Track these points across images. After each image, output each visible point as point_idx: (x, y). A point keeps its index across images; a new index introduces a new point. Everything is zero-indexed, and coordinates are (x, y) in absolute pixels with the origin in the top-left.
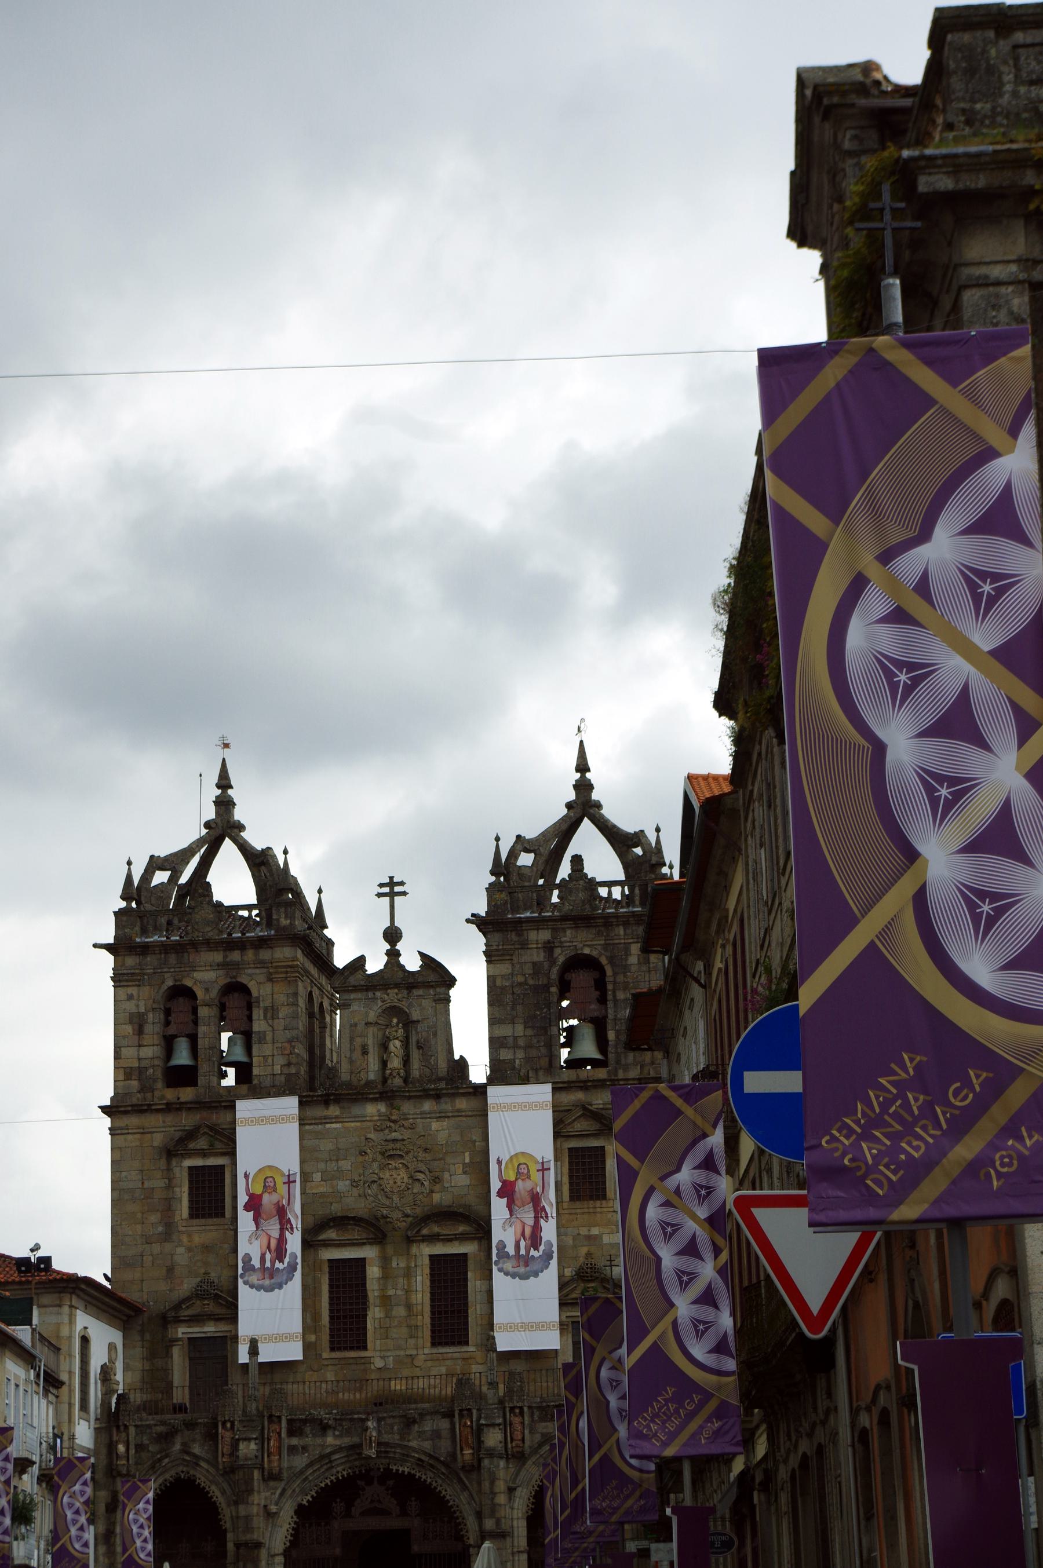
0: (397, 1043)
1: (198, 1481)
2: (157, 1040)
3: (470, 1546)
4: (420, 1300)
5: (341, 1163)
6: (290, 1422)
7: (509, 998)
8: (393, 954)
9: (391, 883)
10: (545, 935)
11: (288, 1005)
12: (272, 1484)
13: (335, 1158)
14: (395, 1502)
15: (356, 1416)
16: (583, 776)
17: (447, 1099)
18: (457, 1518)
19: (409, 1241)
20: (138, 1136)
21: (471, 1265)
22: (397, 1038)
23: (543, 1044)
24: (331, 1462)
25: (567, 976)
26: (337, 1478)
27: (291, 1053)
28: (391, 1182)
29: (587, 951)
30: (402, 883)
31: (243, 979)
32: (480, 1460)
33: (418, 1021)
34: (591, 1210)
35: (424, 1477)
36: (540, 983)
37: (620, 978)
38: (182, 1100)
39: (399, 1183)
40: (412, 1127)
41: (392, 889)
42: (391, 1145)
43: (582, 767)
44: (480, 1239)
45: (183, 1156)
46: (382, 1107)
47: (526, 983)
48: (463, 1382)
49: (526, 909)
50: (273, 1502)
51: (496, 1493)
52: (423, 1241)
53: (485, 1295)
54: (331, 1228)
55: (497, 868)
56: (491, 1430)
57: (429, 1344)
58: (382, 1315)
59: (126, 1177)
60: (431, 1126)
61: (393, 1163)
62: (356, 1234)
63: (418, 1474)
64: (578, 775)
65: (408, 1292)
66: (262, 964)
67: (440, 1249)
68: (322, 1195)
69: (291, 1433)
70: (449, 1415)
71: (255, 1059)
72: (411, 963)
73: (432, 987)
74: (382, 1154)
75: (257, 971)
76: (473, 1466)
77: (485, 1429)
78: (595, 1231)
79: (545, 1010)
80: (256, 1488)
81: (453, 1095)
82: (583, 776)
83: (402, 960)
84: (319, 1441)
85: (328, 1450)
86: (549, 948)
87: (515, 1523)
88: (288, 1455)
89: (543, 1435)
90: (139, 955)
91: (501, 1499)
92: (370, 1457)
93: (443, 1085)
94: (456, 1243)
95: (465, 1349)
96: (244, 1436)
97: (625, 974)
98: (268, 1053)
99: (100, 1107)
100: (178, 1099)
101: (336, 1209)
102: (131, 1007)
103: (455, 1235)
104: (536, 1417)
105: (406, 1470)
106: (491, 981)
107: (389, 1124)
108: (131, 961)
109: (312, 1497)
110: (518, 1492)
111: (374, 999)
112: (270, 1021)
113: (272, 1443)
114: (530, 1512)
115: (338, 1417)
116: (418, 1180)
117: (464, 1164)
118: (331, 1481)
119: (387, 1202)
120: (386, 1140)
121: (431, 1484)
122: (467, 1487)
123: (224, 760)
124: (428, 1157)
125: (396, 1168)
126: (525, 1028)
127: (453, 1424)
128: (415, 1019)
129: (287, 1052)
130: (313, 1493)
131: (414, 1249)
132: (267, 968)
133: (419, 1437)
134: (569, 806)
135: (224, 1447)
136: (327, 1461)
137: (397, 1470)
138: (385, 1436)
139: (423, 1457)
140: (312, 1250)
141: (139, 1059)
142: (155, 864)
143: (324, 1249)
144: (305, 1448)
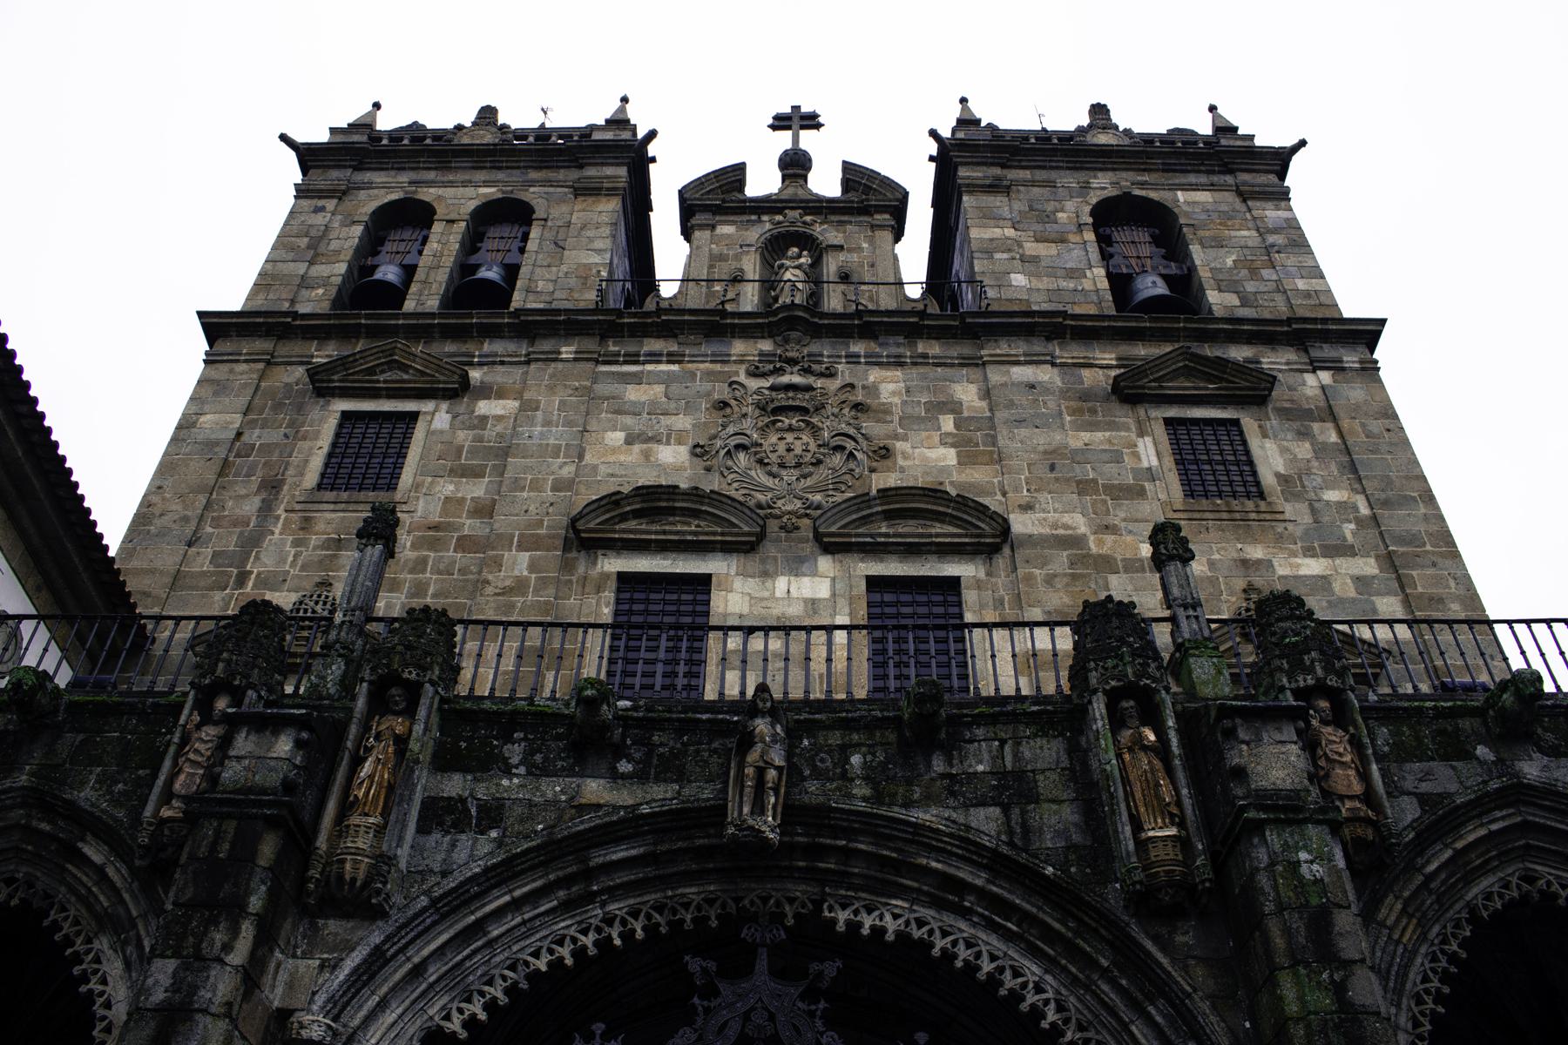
0: (797, 272)
12: (333, 927)
17: (901, 340)
20: (261, 366)
24: (588, 874)
25: (1101, 230)
28: (782, 447)
29: (1137, 192)
33: (841, 248)
34: (1237, 516)
35: (963, 953)
40: (830, 374)
46: (766, 346)
50: (320, 999)
51: (1348, 964)
62: (688, 528)
63: (940, 943)
73: (865, 210)
74: (762, 407)
78: (1256, 552)
88: (423, 829)
89: (1424, 800)
90: (356, 169)
99: (201, 314)
105: (891, 925)
109: (491, 1006)
111: (760, 221)
113: (367, 767)
116: (842, 448)
118: (580, 953)
121: (994, 980)
122: (1160, 987)
127: (1079, 755)
128: (836, 242)
130: (497, 992)
137: (854, 926)
138: (812, 786)
139: (964, 873)
144: (492, 814)
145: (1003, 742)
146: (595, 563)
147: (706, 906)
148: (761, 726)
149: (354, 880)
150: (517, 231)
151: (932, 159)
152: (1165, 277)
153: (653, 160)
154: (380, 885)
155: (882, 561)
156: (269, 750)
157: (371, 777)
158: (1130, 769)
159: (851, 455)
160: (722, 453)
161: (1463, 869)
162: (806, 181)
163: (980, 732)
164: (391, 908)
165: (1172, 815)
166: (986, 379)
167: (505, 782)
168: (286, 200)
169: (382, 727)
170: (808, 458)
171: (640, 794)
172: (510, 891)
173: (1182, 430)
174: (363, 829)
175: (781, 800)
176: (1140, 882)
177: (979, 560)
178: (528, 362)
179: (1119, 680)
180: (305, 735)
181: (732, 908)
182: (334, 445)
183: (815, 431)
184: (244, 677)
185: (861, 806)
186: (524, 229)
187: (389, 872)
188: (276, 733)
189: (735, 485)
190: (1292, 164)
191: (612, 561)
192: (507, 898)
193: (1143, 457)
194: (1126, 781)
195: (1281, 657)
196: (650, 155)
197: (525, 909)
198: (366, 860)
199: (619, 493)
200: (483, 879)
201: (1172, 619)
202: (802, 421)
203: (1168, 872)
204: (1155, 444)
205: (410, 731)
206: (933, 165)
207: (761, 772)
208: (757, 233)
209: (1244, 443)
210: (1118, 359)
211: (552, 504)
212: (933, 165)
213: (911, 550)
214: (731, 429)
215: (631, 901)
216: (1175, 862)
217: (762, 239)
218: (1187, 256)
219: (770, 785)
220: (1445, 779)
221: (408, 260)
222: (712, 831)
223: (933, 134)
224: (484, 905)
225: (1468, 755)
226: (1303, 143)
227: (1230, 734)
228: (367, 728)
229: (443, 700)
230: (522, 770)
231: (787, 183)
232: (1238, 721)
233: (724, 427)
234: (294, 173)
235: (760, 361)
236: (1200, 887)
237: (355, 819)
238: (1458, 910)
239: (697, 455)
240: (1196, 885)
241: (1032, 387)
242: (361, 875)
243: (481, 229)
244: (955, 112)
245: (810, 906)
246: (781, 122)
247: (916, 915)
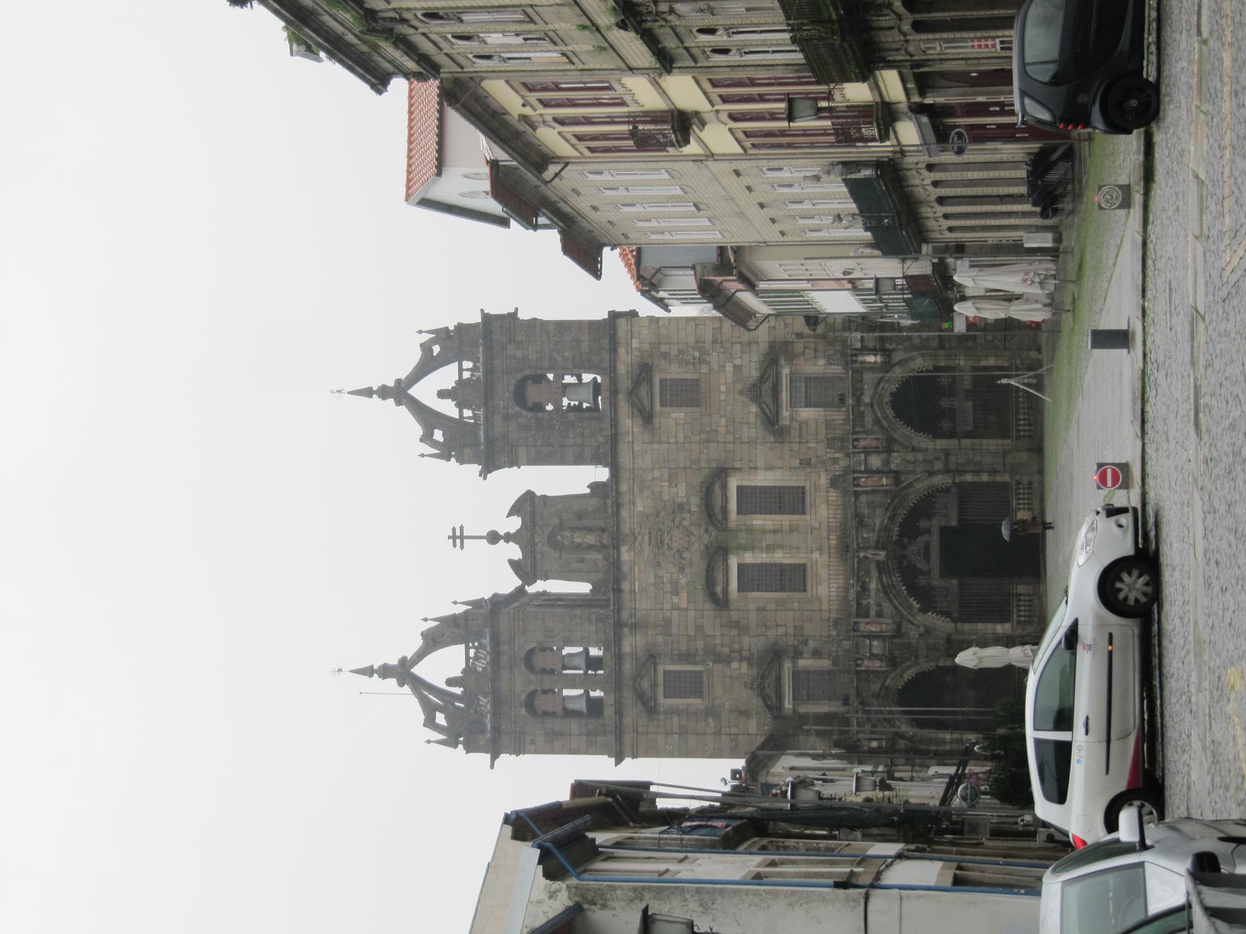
0: (576, 535)
1: (900, 687)
3: (954, 482)
4: (771, 523)
5: (665, 580)
6: (858, 616)
8: (508, 538)
9: (454, 537)
10: (498, 420)
13: (661, 585)
14: (919, 538)
15: (856, 566)
16: (375, 392)
17: (621, 498)
18: (933, 491)
19: (726, 530)
21: (745, 483)
22: (572, 536)
24: (889, 585)
25: (530, 404)
26: (901, 581)
28: (681, 541)
29: (512, 388)
30: (454, 530)
31: (522, 654)
32: (891, 472)
35: (902, 516)
38: (613, 703)
39: (683, 536)
41: (458, 537)
42: (653, 542)
43: (368, 392)
44: (727, 476)
45: (655, 700)
46: (624, 549)
48: (834, 482)
49: (477, 435)
53: (768, 473)
55: (445, 455)
57: (804, 516)
58: (781, 551)
61: (667, 539)
63: (900, 520)
64: (375, 396)
65: (764, 532)
67: (733, 506)
68: (689, 595)
69: (867, 615)
70: (857, 494)
72: (515, 524)
74: (659, 548)
77: (869, 467)
78: (723, 388)
79: (555, 422)
80: (906, 641)
81: (618, 494)
82: (375, 392)
83: (512, 531)
84: (873, 593)
85: (879, 586)
86: (507, 417)
87: (938, 447)
88: (883, 617)
89: (874, 424)
91: (920, 456)
92: (887, 556)
93: (609, 501)
95: (807, 489)
96: (868, 650)
99: (616, 765)
100: (612, 705)
101: (700, 586)
104: (861, 429)
105: (897, 528)
106: (531, 462)
107: (637, 543)
110: (915, 443)
113: (873, 629)
114: (930, 436)
115: (856, 579)
117: (670, 487)
119: (696, 545)
123: (351, 671)
124: (663, 513)
125: (671, 539)
126: (568, 437)
127: (863, 492)
128: (558, 522)
132: (514, 635)
134: (398, 403)
135: (876, 665)
137: (897, 535)
141: (581, 735)
142: (430, 722)
143: (729, 596)
148: (862, 555)
161: (886, 417)
220: (869, 419)
225: (863, 413)
226: (482, 310)
234: (504, 759)
237: (884, 629)
238: (893, 420)
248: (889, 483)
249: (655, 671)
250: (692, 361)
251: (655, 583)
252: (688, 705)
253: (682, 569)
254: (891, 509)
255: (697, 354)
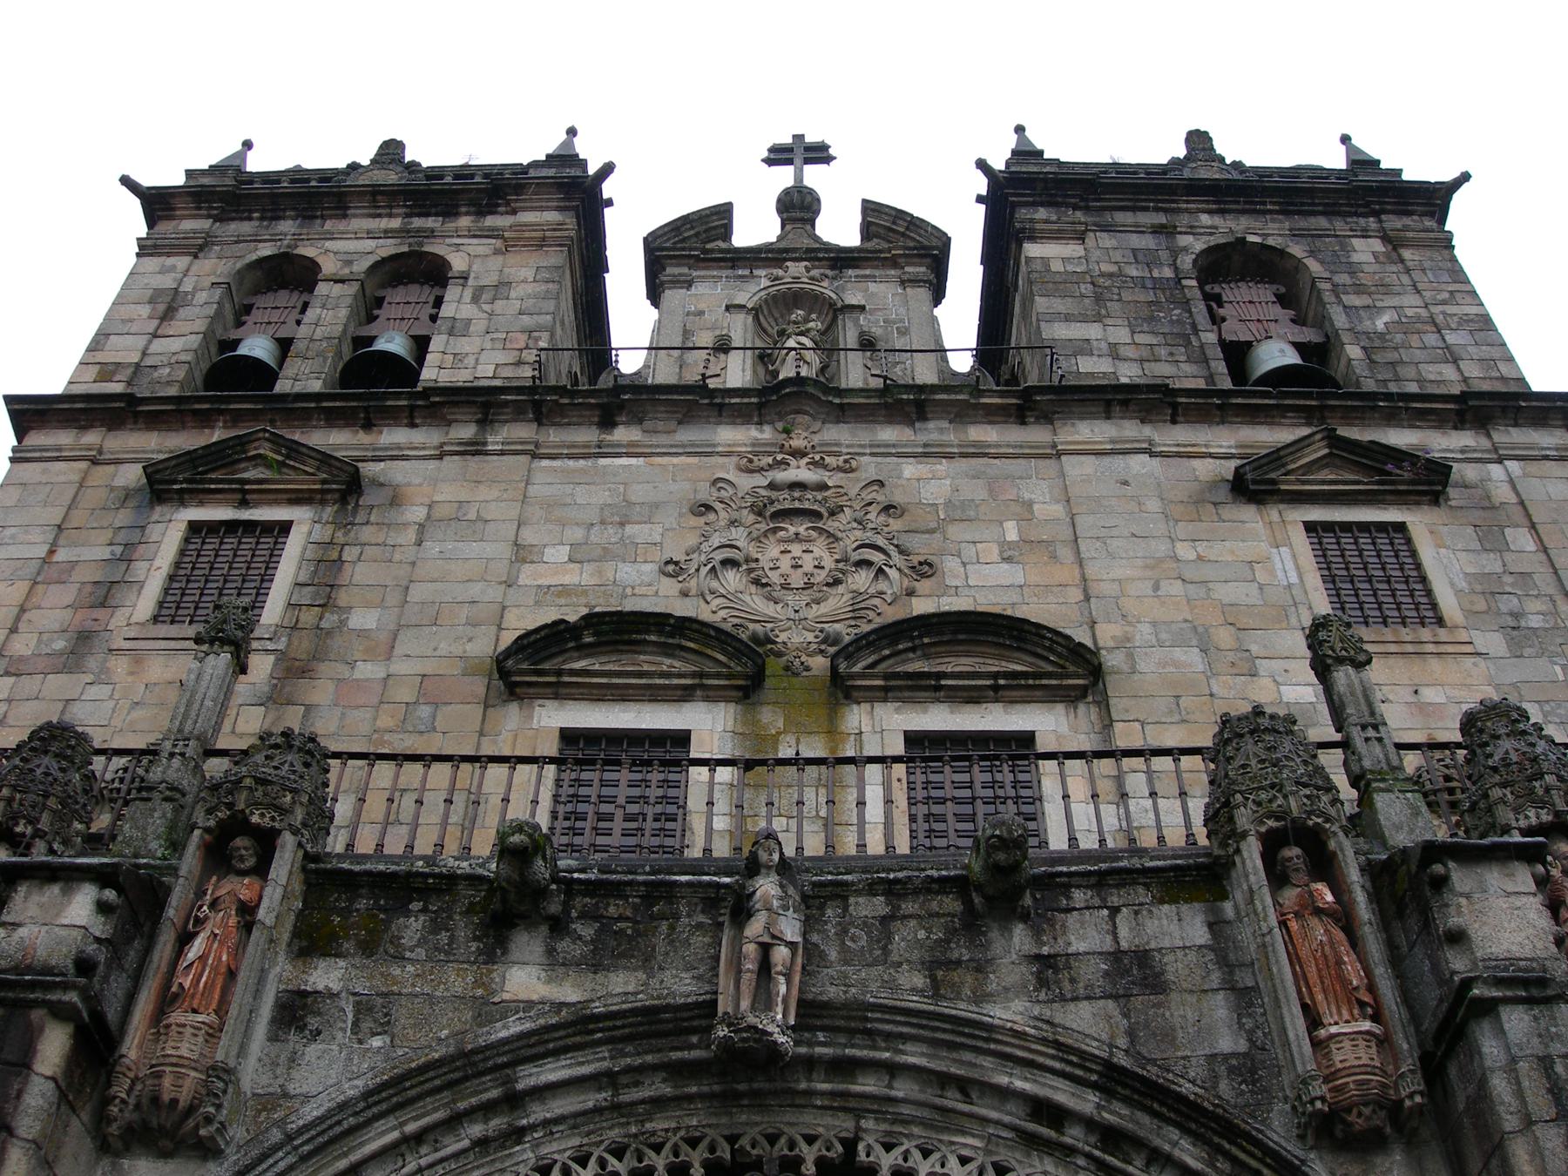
2: (200, 325)
5: (629, 529)
7: (1086, 289)
11: (535, 281)
17: (945, 424)
20: (84, 465)
22: (802, 334)
23: (1183, 358)
24: (514, 1100)
27: (527, 348)
28: (785, 563)
29: (1251, 239)
33: (862, 308)
34: (1409, 648)
36: (1156, 274)
37: (1342, 278)
40: (846, 469)
42: (785, 494)
44: (1071, 697)
46: (766, 434)
47: (1120, 274)
52: (885, 694)
54: (584, 650)
56: (1494, 877)
59: (13, 537)
60: (901, 472)
66: (493, 233)
68: (564, 591)
71: (428, 356)
73: (893, 263)
75: (475, 241)
76: (1394, 1109)
77: (1461, 878)
78: (1430, 695)
88: (273, 1038)
90: (217, 219)
94: (997, 709)
97: (1352, 274)
98: (467, 349)
102: (168, 282)
103: (996, 675)
108: (191, 225)
111: (752, 276)
112: (486, 307)
116: (869, 563)
117: (1004, 545)
119: (770, 610)
120: (772, 486)
124: (896, 525)
126: (1133, 333)
128: (854, 302)
129: (522, 345)
131: (856, 717)
133: (1042, 983)
136: (494, 1093)
139: (1062, 1094)
140: (513, 708)
141: (144, 354)
145: (1115, 911)
146: (532, 718)
147: (685, 1148)
149: (174, 1102)
150: (427, 294)
151: (980, 199)
152: (1299, 347)
153: (609, 203)
154: (212, 1110)
155: (925, 711)
156: (58, 915)
157: (202, 958)
158: (1298, 941)
159: (880, 571)
160: (704, 570)
162: (813, 226)
163: (1079, 897)
164: (227, 1143)
165: (1362, 1004)
166: (1063, 475)
167: (396, 971)
168: (126, 258)
169: (222, 892)
170: (821, 576)
171: (589, 985)
172: (402, 1124)
173: (1329, 540)
174: (189, 1030)
175: (795, 992)
176: (1323, 1099)
177: (1060, 708)
178: (440, 457)
179: (1278, 819)
180: (110, 895)
181: (725, 1152)
182: (177, 565)
183: (833, 538)
184: (30, 822)
185: (915, 1002)
186: (437, 291)
187: (225, 1092)
188: (67, 892)
189: (723, 613)
190: (1453, 204)
191: (551, 714)
192: (395, 1135)
193: (1280, 574)
194: (1294, 958)
195: (1504, 785)
196: (605, 196)
197: (424, 1150)
198: (193, 1074)
199: (563, 621)
200: (362, 1105)
201: (1345, 745)
202: (813, 528)
203: (1360, 1083)
204: (1294, 556)
205: (261, 898)
206: (982, 208)
207: (765, 949)
208: (750, 292)
209: (1414, 553)
210: (1237, 447)
211: (470, 640)
212: (983, 207)
213: (972, 697)
214: (716, 540)
215: (576, 1141)
216: (1367, 1069)
217: (756, 298)
218: (1322, 321)
219: (779, 968)
221: (283, 333)
222: (695, 1039)
223: (982, 165)
224: (362, 1144)
226: (1465, 177)
227: (1441, 883)
228: (200, 893)
229: (308, 857)
230: (421, 953)
231: (788, 227)
232: (1451, 864)
233: (706, 537)
234: (135, 223)
235: (756, 454)
236: (1408, 1103)
237: (177, 1017)
239: (669, 575)
240: (1402, 1101)
241: (1126, 483)
242: (184, 1099)
243: (380, 293)
244: (1011, 141)
245: (840, 1149)
246: (779, 156)
247: (995, 1158)
248: (1343, 1055)
249: (297, 499)
250: (1504, 609)
251: (630, 504)
252: (141, 584)
253: (672, 568)
254: (1117, 1115)
255: (1535, 622)
